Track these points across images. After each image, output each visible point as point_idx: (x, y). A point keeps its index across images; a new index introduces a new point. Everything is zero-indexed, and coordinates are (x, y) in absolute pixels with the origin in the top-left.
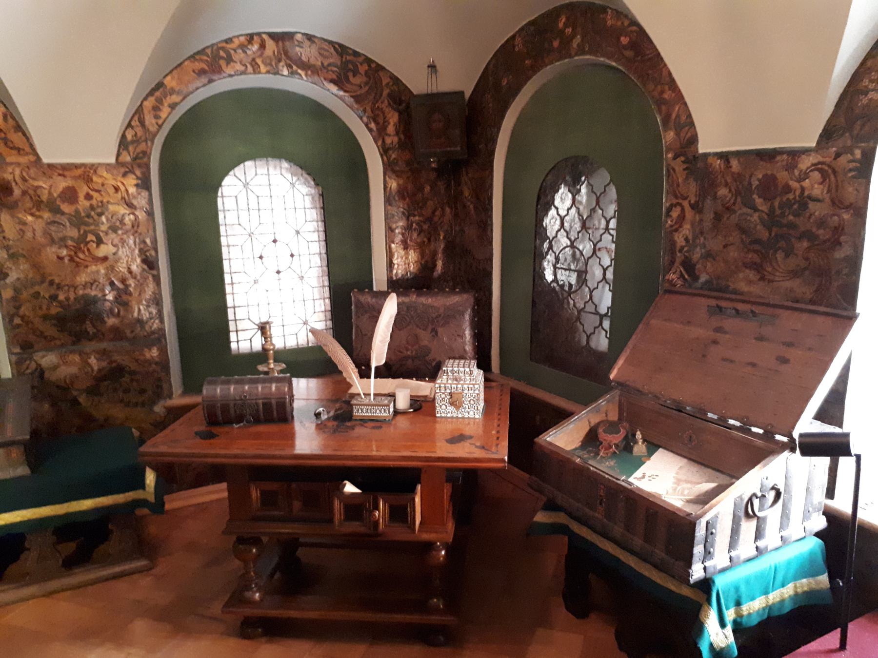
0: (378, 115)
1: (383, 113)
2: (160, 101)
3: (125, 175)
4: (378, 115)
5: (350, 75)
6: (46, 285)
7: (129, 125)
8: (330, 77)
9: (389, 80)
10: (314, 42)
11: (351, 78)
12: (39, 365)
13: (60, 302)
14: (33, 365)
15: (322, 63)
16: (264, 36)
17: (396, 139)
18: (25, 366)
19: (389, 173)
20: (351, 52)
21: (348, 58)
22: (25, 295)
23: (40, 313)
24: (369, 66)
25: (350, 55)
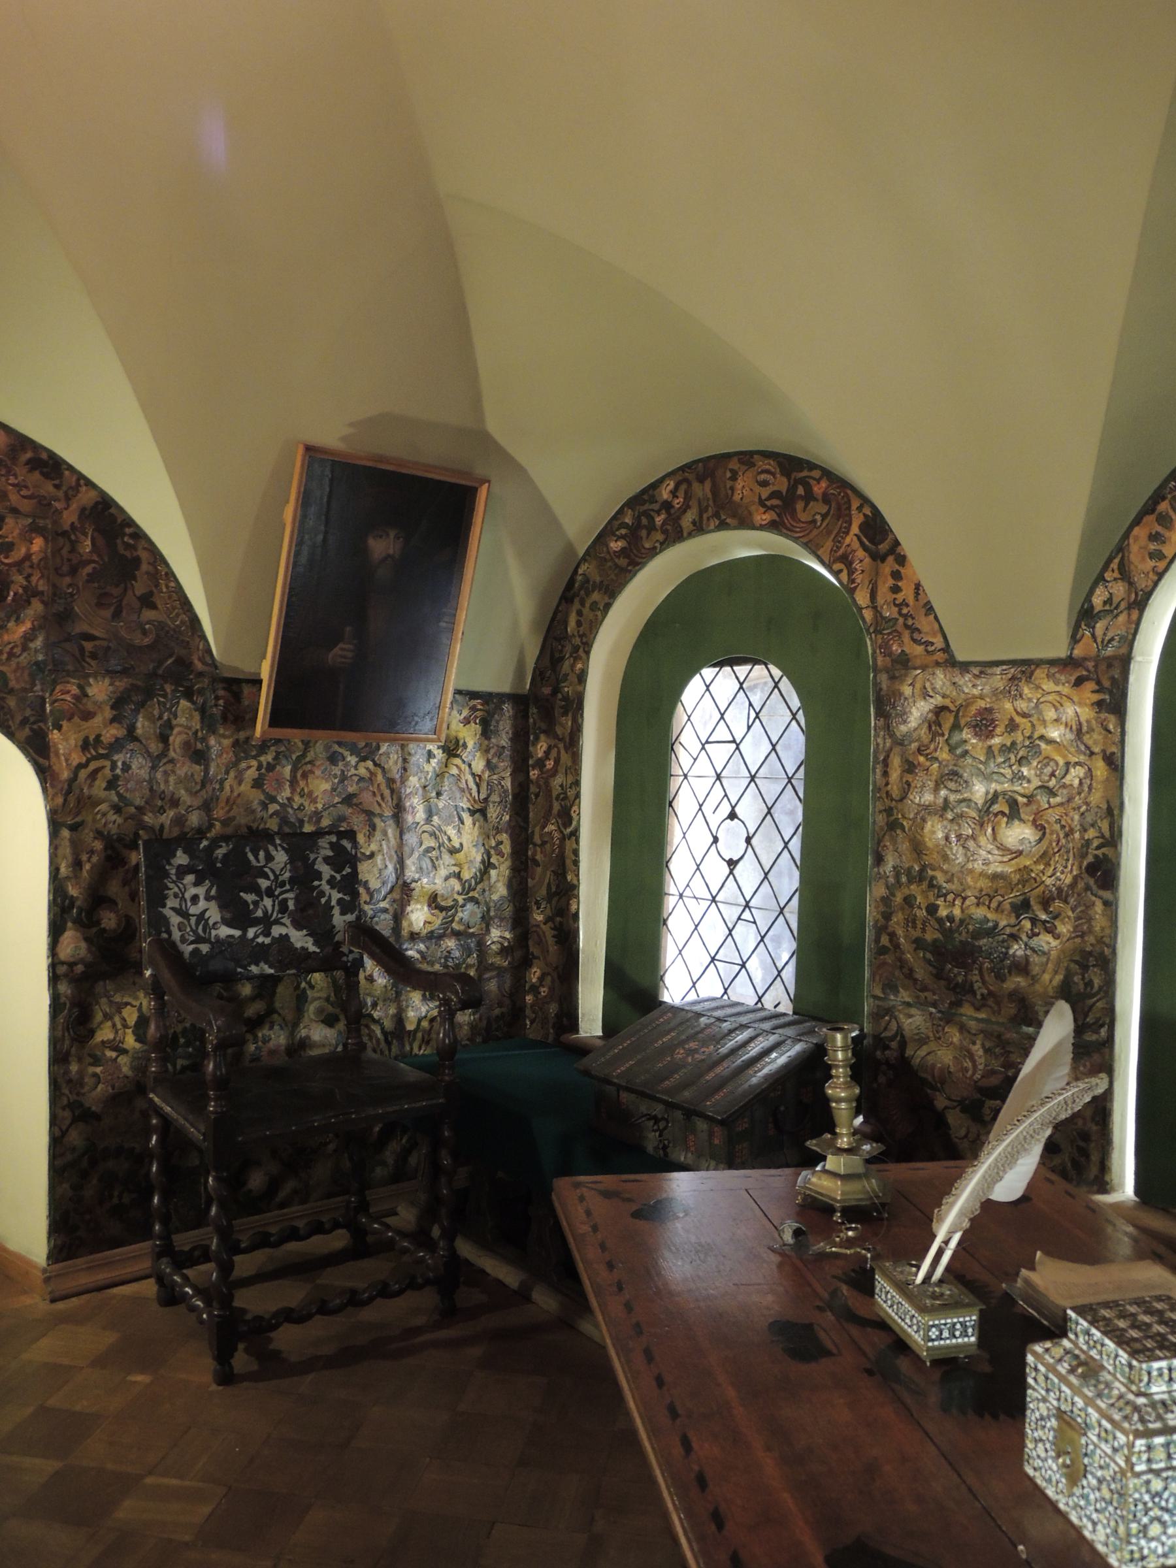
3: (1079, 682)
6: (925, 885)
7: (1100, 579)
12: (899, 1027)
13: (940, 921)
18: (883, 1025)
22: (899, 898)
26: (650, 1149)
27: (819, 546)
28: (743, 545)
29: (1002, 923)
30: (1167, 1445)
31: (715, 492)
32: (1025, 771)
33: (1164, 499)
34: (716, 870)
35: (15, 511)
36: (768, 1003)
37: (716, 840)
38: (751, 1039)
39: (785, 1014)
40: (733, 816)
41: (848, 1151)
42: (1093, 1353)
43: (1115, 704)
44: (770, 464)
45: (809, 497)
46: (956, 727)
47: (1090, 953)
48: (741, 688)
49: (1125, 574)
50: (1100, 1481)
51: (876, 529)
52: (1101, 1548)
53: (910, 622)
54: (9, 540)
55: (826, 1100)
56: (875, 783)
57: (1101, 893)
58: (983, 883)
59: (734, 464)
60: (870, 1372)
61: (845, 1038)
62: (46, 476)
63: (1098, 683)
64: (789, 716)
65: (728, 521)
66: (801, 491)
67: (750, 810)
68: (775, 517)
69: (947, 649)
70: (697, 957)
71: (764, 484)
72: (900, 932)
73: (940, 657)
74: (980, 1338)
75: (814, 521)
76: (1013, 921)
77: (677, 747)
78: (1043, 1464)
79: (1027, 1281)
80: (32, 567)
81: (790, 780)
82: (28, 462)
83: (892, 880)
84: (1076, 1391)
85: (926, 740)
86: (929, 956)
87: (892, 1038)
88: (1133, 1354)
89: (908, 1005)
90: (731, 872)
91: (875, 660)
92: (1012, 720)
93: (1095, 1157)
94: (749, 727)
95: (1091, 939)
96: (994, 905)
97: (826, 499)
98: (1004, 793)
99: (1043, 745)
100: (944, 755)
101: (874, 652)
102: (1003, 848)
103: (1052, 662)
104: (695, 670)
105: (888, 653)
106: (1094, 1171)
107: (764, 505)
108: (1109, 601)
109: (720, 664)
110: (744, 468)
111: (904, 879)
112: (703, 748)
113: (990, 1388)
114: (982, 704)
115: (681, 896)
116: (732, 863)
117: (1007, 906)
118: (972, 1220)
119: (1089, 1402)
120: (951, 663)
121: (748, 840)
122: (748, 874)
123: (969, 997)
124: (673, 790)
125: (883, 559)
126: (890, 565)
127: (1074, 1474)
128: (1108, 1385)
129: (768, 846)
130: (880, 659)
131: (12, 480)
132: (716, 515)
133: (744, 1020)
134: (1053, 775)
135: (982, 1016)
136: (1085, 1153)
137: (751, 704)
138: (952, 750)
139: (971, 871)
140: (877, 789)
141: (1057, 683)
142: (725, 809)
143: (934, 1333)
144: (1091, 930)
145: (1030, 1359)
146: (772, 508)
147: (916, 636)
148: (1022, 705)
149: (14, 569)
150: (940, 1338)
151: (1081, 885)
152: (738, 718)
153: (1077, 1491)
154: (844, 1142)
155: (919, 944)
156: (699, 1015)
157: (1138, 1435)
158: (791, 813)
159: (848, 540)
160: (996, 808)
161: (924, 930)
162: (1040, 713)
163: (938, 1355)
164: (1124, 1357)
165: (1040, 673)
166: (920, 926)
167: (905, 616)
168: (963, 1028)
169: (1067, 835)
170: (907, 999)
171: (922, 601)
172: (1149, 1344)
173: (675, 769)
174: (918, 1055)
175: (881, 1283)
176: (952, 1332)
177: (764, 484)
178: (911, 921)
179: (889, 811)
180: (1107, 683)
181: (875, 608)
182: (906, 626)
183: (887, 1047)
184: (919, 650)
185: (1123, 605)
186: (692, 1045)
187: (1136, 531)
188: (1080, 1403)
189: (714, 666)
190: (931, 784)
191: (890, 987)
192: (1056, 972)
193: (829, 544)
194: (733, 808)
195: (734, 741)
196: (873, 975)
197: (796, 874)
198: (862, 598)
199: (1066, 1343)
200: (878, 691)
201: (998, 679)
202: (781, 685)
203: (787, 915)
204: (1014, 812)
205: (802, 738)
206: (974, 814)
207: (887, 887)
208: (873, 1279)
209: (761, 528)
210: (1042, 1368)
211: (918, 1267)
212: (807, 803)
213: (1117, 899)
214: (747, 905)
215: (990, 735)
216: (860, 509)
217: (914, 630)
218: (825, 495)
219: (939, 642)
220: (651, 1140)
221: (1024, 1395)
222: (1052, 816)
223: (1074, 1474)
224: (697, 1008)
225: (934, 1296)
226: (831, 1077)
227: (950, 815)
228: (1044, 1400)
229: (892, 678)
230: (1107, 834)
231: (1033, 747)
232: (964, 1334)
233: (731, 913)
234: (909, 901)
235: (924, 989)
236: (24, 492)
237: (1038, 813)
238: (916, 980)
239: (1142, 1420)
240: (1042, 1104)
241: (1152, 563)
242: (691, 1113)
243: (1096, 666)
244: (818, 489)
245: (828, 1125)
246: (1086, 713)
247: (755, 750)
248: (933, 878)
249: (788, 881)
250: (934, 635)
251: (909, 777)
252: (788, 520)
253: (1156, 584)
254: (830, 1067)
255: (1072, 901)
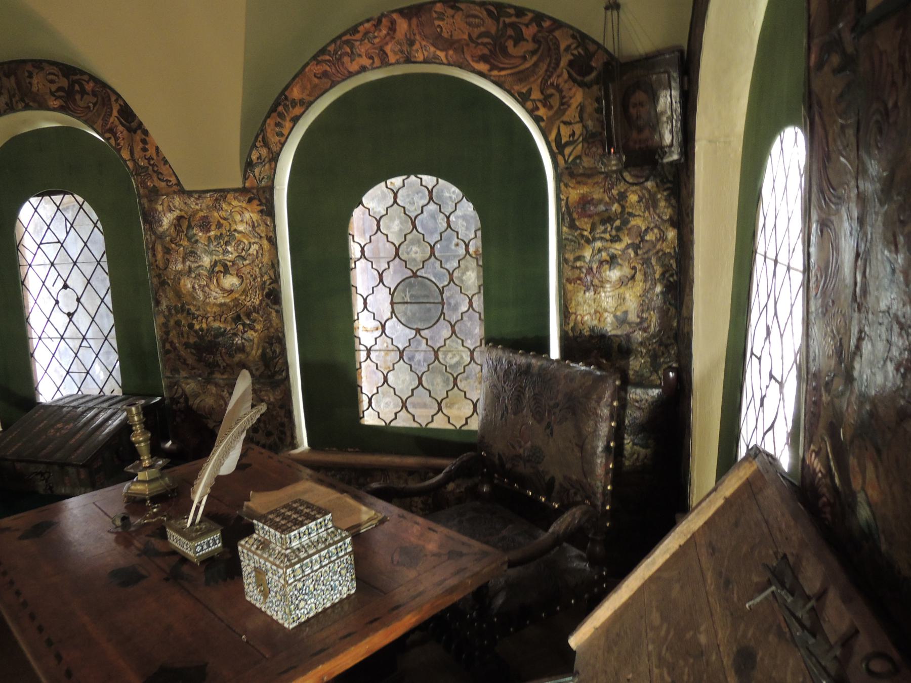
0: (551, 95)
1: (560, 91)
2: (281, 116)
3: (250, 201)
4: (551, 95)
5: (510, 43)
6: (185, 314)
8: (480, 53)
9: (570, 41)
10: (459, 9)
11: (511, 49)
12: (183, 391)
13: (196, 332)
14: (180, 391)
15: (470, 35)
16: (395, 16)
17: (578, 129)
19: (566, 179)
20: (512, 11)
21: (507, 20)
22: (172, 323)
23: (184, 340)
24: (539, 25)
25: (510, 16)
26: (41, 490)
27: (94, 123)
28: (47, 120)
29: (228, 328)
30: (301, 567)
31: (18, 83)
32: (229, 248)
33: (280, 104)
34: (60, 320)
36: (107, 391)
37: (57, 302)
38: (97, 415)
39: (116, 396)
40: (65, 286)
41: (151, 467)
42: (266, 537)
43: (269, 211)
44: (55, 70)
45: (83, 92)
46: (190, 227)
47: (273, 337)
48: (58, 209)
49: (266, 144)
50: (276, 593)
51: (127, 114)
52: (281, 621)
53: (156, 169)
55: (132, 444)
56: (149, 261)
57: (274, 307)
58: (215, 309)
59: (29, 67)
60: (167, 579)
61: (137, 408)
63: (260, 200)
64: (92, 225)
65: (31, 104)
66: (77, 87)
67: (77, 282)
68: (63, 103)
69: (179, 183)
70: (57, 373)
71: (52, 82)
72: (176, 341)
73: (175, 188)
74: (223, 543)
75: (89, 107)
76: (234, 326)
77: (21, 248)
78: (253, 594)
79: (248, 507)
81: (99, 263)
83: (166, 313)
84: (261, 557)
85: (174, 236)
86: (193, 351)
87: (181, 397)
88: (282, 533)
89: (186, 378)
90: (71, 320)
91: (138, 191)
92: (219, 222)
93: (288, 434)
94: (68, 233)
95: (272, 330)
96: (223, 319)
97: (94, 94)
98: (220, 261)
99: (236, 235)
100: (185, 243)
101: (137, 186)
102: (223, 290)
103: (235, 190)
104: (26, 199)
105: (145, 187)
106: (289, 440)
107: (54, 96)
108: (259, 158)
109: (42, 195)
110: (36, 71)
111: (173, 312)
112: (39, 247)
113: (226, 567)
114: (201, 214)
115: (40, 338)
116: (70, 315)
117: (229, 319)
118: (212, 488)
119: (266, 560)
120: (182, 192)
121: (78, 300)
122: (82, 320)
123: (217, 369)
124: (23, 275)
125: (135, 132)
126: (139, 136)
127: (265, 594)
128: (274, 549)
129: (91, 302)
130: (141, 191)
132: (22, 100)
133: (91, 404)
134: (243, 249)
135: (225, 377)
136: (283, 433)
137: (66, 219)
138: (189, 240)
139: (209, 303)
140: (151, 264)
141: (239, 201)
142: (60, 284)
143: (199, 549)
144: (271, 326)
145: (240, 548)
146: (60, 97)
147: (160, 176)
148: (223, 214)
150: (202, 550)
151: (264, 304)
152: (59, 228)
153: (268, 600)
154: (146, 463)
155: (187, 345)
156: (61, 407)
157: (287, 567)
158: (102, 282)
159: (111, 120)
160: (217, 269)
161: (188, 338)
162: (233, 217)
163: (203, 559)
164: (278, 534)
165: (230, 196)
166: (185, 336)
167: (153, 165)
168: (216, 385)
169: (254, 280)
170: (185, 375)
171: (161, 158)
172: (289, 525)
173: (22, 261)
174: (195, 403)
175: (170, 532)
176: (212, 543)
177: (52, 82)
178: (181, 334)
179: (159, 276)
180: (264, 201)
181: (134, 160)
182: (154, 171)
183: (179, 402)
184: (163, 184)
185: (267, 160)
186: (59, 426)
187: (268, 121)
188: (262, 561)
189: (38, 196)
190: (181, 259)
191: (175, 370)
192: (258, 349)
193: (100, 122)
194: (65, 282)
195: (59, 242)
196: (164, 366)
197: (112, 316)
198: (125, 154)
199: (255, 536)
200: (143, 209)
201: (208, 200)
202: (84, 207)
203: (110, 340)
204: (226, 271)
205: (102, 237)
206: (206, 273)
207: (165, 317)
208: (166, 532)
209: (54, 110)
210: (245, 551)
211: (188, 518)
212: (111, 274)
213: (282, 309)
214: (84, 338)
215: (209, 230)
216: (116, 100)
217: (158, 173)
218: (93, 91)
219: (173, 180)
220: (41, 487)
221: (240, 565)
222: (246, 270)
223: (265, 594)
224: (60, 403)
225: (197, 531)
226: (133, 431)
227: (193, 275)
228: (249, 565)
229: (150, 201)
230: (273, 277)
231: (231, 236)
232: (215, 543)
233: (75, 344)
234: (178, 323)
235: (193, 368)
237: (238, 270)
238: (188, 365)
239: (289, 560)
240: (237, 424)
241: (278, 138)
242: (63, 465)
243: (258, 191)
244: (89, 87)
245: (135, 455)
246: (255, 217)
247: (74, 247)
248: (189, 310)
249: (107, 320)
250: (171, 176)
251: (168, 256)
252: (71, 106)
253: (281, 149)
254: (131, 426)
255: (261, 312)
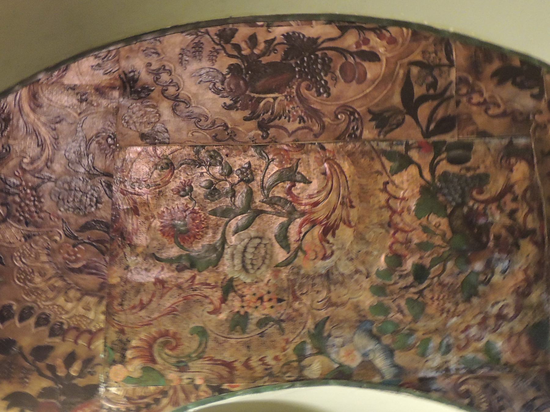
35: (483, 134)
54: (482, 170)
62: (521, 86)
80: (515, 199)
82: (494, 74)
131: (476, 98)
149: (493, 206)
236: (493, 111)
